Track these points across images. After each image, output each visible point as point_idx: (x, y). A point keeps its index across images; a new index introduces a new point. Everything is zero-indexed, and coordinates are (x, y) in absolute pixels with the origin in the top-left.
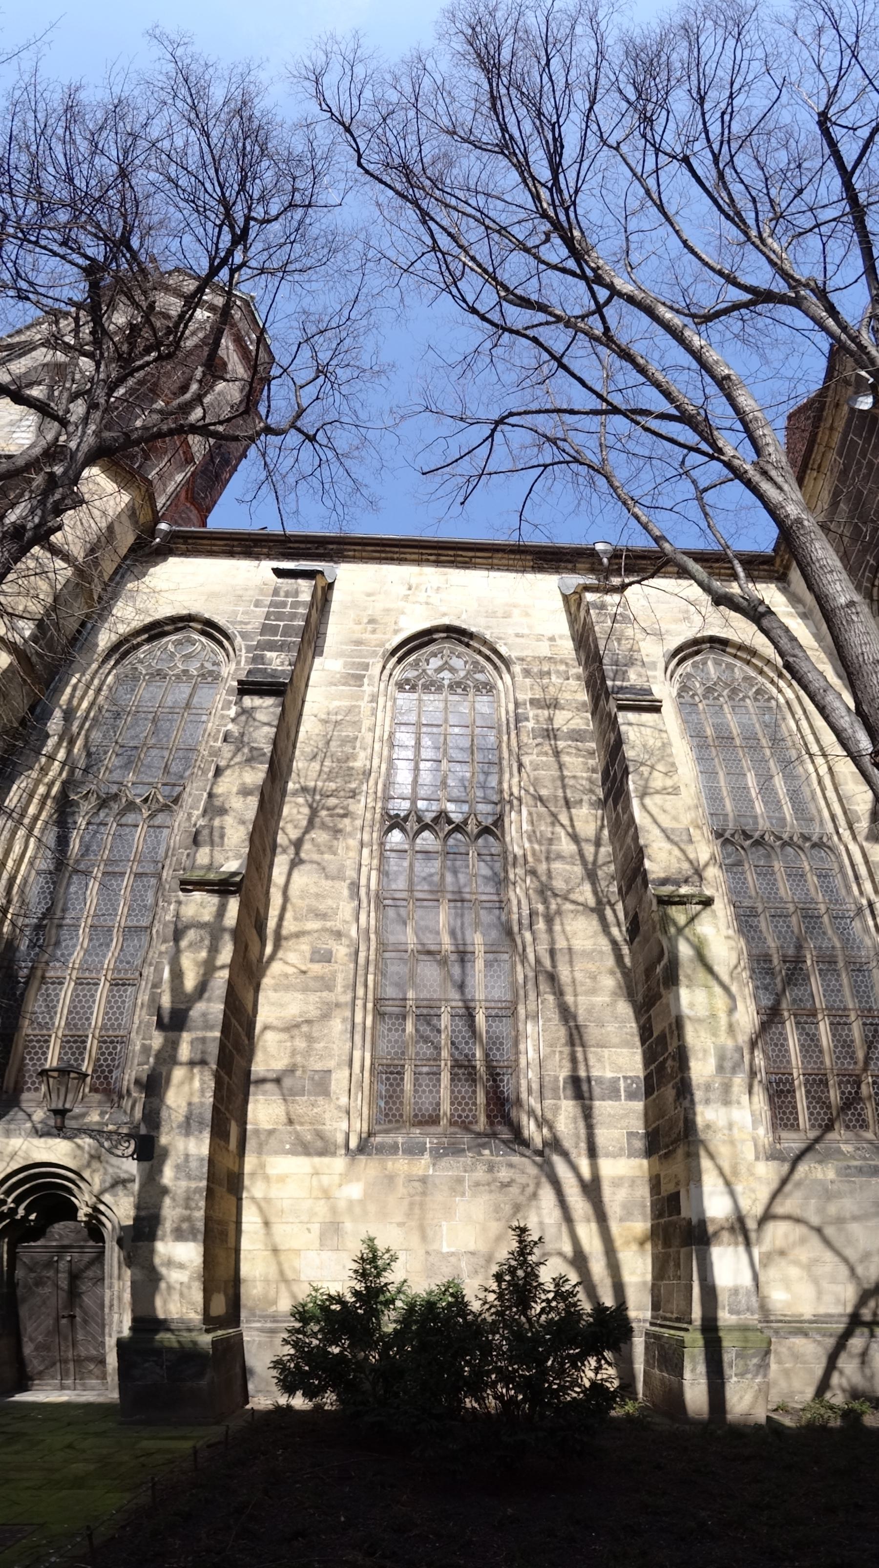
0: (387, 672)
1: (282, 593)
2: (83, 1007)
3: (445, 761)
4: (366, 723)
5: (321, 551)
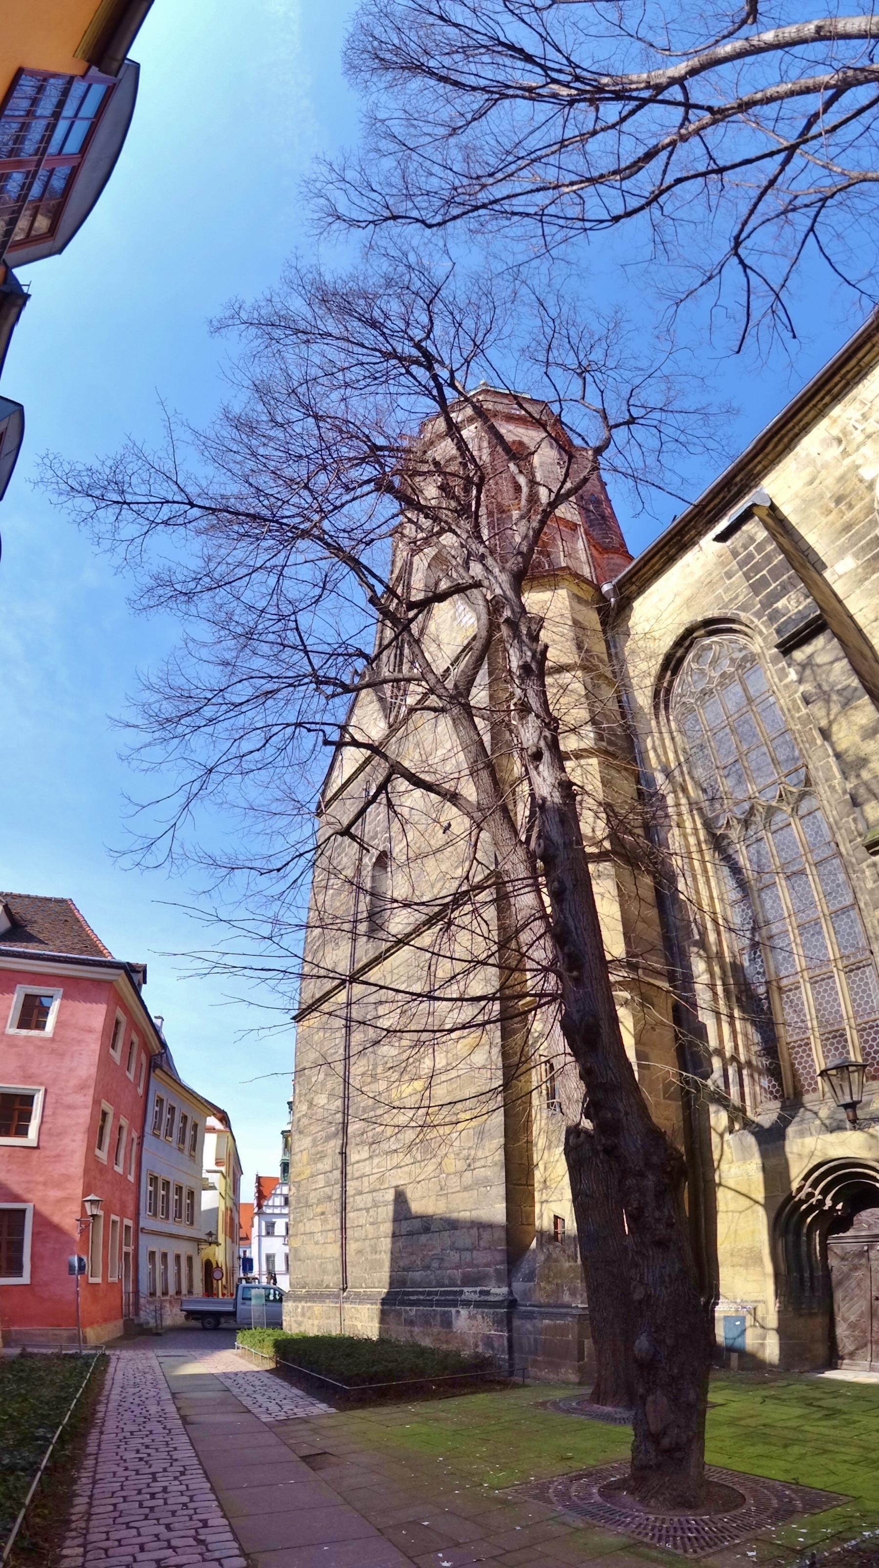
1: (741, 550)
2: (828, 1002)
5: (734, 490)
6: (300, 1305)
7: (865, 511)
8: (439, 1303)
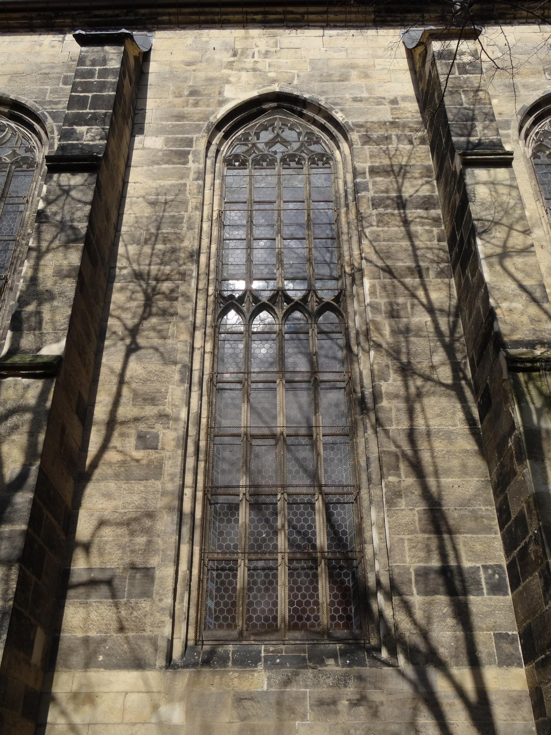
0: (213, 148)
3: (278, 238)
4: (193, 202)
5: (131, 17)
7: (202, 115)
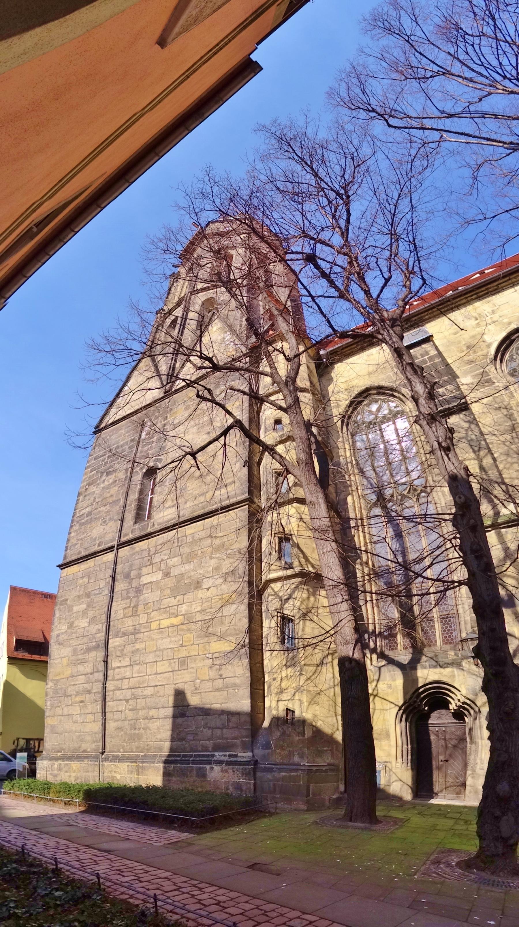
6: (56, 763)
8: (194, 762)
